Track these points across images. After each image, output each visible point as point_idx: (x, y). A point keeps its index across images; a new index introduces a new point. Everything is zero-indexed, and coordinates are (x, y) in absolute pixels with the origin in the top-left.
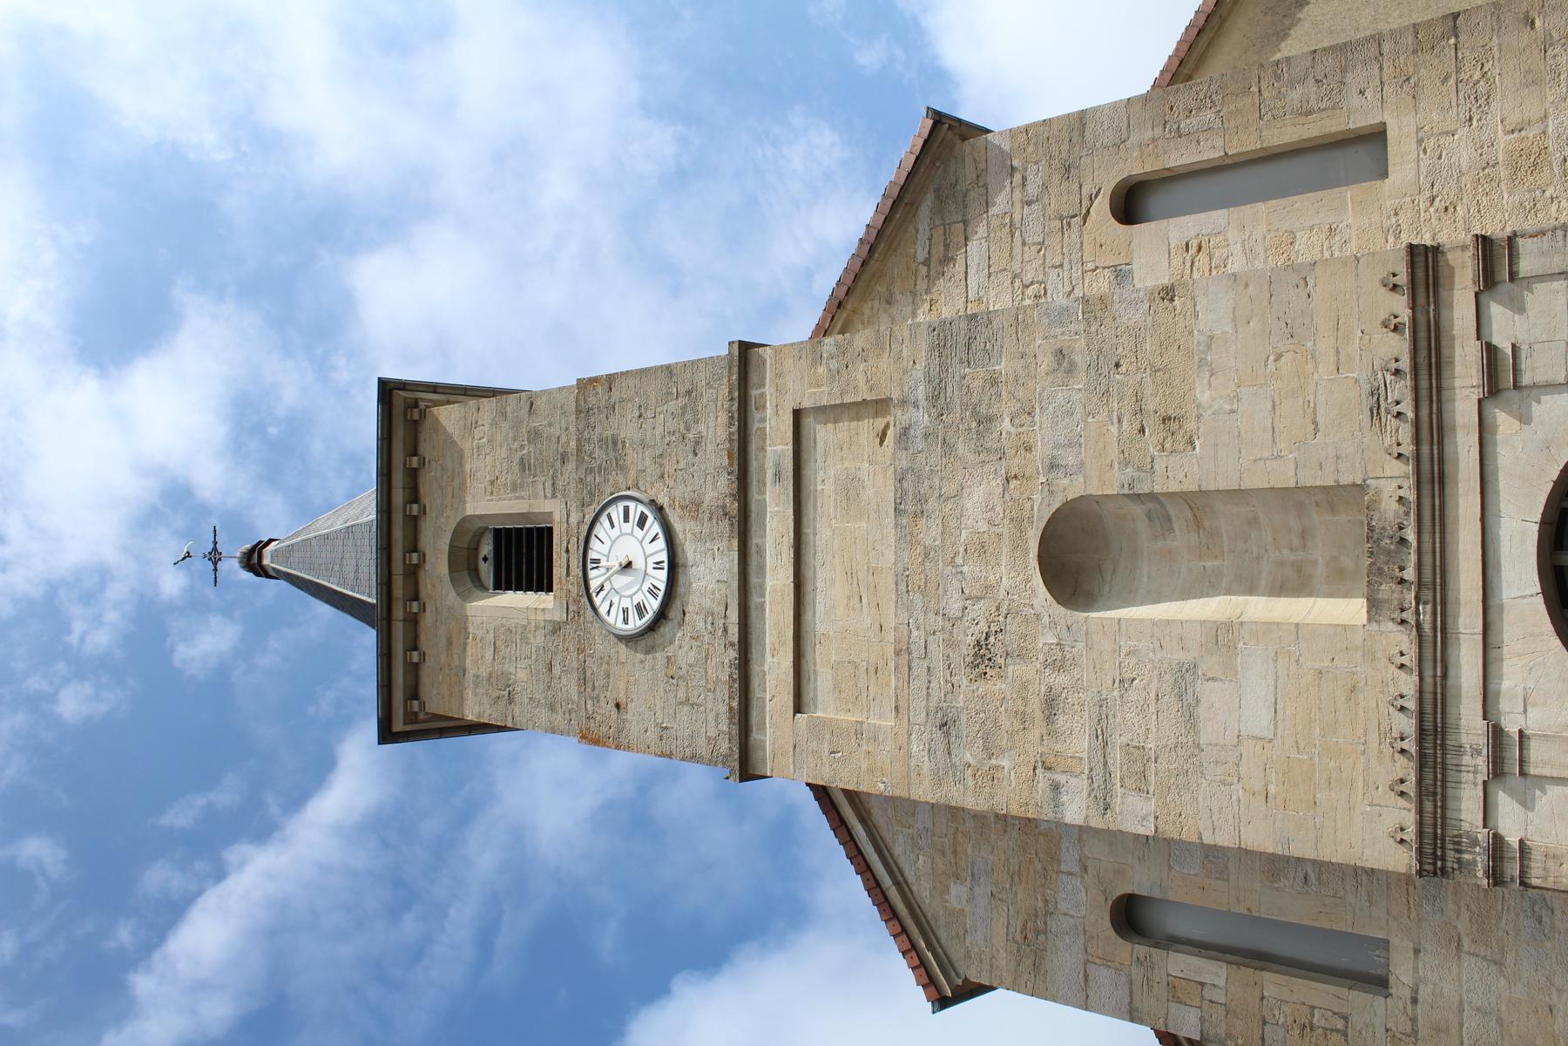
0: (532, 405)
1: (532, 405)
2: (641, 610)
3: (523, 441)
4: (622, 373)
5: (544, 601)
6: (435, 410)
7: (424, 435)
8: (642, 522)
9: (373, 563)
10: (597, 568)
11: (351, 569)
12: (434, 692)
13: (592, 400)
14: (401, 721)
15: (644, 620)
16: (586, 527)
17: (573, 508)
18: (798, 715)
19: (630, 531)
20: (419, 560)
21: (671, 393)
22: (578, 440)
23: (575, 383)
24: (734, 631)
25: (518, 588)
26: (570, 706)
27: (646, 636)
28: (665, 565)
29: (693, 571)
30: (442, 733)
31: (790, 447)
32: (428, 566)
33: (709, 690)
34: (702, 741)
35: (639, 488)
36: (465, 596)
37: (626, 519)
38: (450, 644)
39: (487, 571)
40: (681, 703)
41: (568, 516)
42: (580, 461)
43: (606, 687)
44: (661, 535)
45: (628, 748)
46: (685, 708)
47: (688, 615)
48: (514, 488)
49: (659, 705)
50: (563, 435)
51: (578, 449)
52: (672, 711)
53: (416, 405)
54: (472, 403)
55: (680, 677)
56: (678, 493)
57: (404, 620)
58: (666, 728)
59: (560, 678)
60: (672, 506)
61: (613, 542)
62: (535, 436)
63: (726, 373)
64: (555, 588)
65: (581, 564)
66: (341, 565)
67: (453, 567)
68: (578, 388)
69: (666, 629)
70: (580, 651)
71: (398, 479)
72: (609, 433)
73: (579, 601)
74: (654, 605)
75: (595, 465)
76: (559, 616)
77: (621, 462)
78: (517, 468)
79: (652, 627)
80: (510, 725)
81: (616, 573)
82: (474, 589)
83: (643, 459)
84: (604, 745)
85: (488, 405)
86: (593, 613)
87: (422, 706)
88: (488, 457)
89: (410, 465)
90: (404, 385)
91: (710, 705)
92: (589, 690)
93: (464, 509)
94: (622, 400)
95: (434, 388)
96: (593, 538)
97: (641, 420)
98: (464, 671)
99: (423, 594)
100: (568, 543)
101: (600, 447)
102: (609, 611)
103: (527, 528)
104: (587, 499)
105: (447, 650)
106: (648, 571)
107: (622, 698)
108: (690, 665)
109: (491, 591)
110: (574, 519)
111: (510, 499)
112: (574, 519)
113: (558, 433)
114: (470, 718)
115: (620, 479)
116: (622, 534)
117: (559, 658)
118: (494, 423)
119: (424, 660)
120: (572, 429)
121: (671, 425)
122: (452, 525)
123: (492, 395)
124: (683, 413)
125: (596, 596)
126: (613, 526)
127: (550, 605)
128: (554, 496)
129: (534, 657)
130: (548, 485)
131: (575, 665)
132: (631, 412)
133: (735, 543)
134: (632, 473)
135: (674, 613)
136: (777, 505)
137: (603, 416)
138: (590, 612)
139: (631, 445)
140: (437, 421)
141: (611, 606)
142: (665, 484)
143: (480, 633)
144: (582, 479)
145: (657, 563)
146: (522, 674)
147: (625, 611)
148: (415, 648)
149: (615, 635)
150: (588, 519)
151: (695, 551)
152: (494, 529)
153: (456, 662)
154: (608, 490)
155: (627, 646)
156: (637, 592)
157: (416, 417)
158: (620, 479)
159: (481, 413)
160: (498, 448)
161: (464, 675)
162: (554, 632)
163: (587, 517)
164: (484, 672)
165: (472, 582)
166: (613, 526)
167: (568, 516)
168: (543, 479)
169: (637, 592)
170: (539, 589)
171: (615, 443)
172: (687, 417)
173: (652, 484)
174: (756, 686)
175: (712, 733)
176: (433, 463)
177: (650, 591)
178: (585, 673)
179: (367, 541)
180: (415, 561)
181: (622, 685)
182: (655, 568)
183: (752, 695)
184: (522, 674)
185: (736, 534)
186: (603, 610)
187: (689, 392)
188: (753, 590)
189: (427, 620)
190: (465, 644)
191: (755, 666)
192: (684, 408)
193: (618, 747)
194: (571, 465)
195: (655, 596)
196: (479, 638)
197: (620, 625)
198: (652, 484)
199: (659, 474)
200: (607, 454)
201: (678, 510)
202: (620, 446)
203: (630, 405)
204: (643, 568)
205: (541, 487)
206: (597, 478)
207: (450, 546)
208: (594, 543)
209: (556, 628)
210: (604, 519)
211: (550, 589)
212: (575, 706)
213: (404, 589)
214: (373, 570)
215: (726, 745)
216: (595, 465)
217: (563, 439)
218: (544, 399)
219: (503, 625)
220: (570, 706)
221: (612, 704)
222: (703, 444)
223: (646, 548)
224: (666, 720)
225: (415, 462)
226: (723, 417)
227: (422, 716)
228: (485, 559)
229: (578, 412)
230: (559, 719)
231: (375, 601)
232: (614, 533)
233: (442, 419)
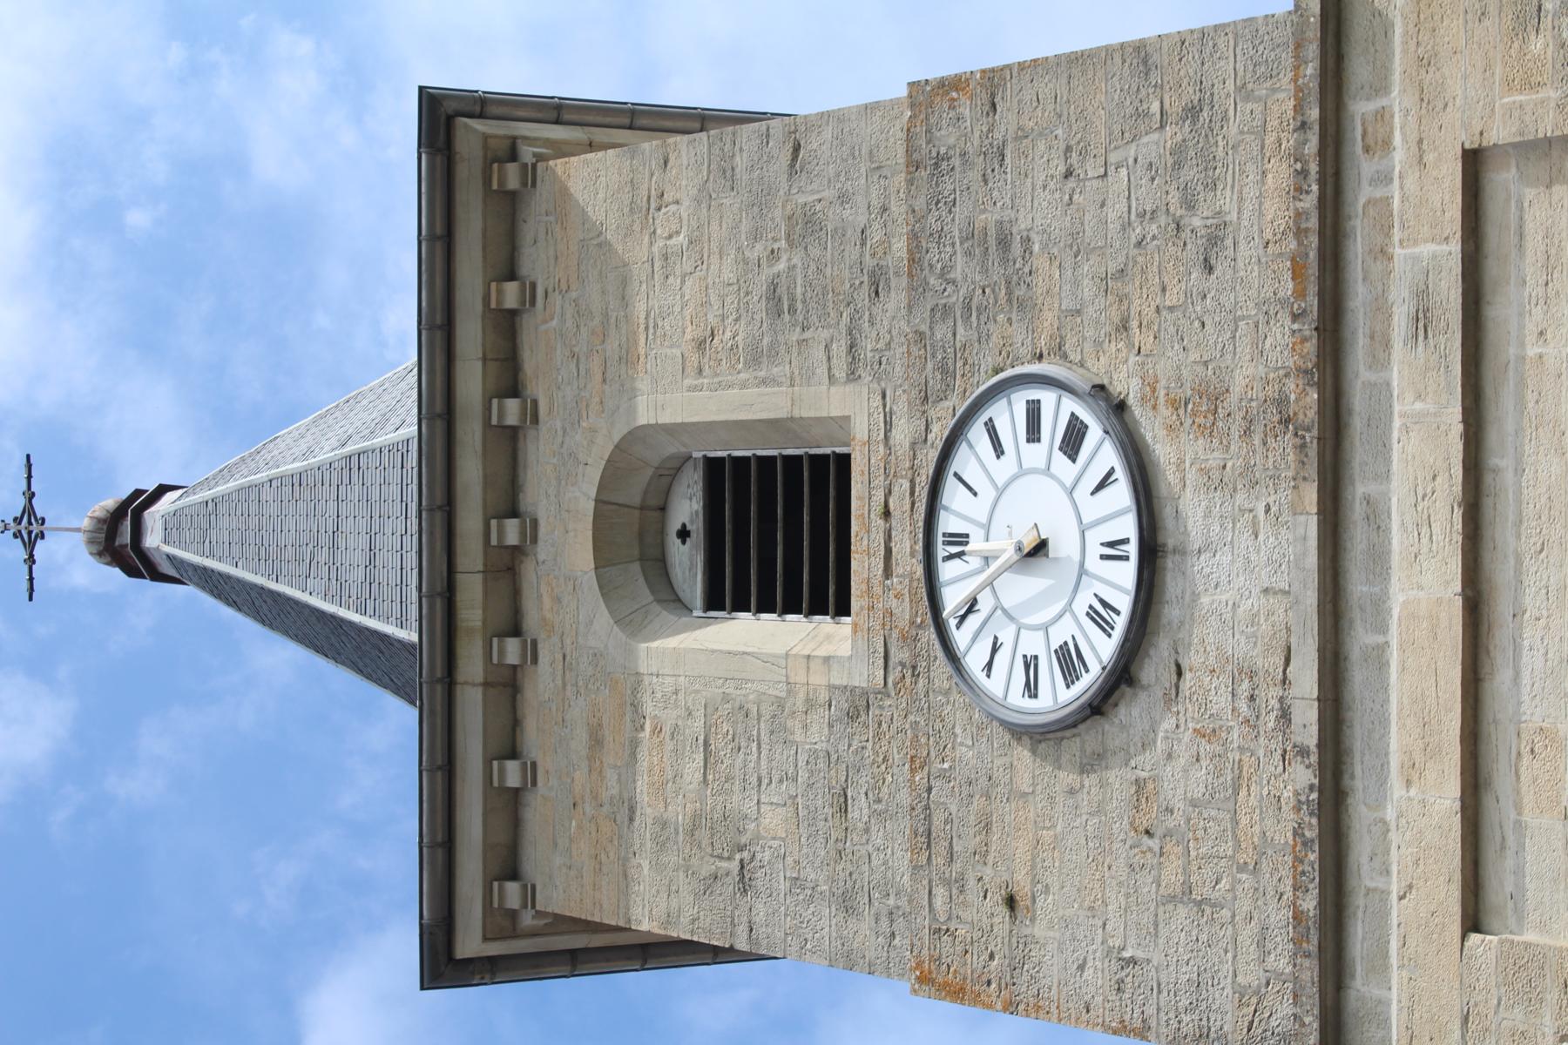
0: (797, 149)
1: (797, 149)
2: (1069, 661)
3: (775, 240)
4: (1022, 66)
5: (829, 637)
6: (558, 165)
7: (530, 229)
8: (1073, 440)
9: (411, 543)
10: (960, 555)
11: (359, 558)
12: (558, 860)
13: (947, 137)
15: (1079, 687)
16: (934, 455)
17: (900, 407)
18: (1475, 938)
19: (1042, 465)
20: (523, 534)
21: (1147, 114)
22: (914, 236)
23: (903, 92)
24: (1307, 719)
25: (766, 606)
26: (891, 902)
27: (1082, 727)
28: (1132, 549)
29: (1201, 566)
30: (575, 962)
31: (1455, 247)
32: (543, 551)
33: (1242, 868)
34: (1223, 997)
35: (1065, 356)
36: (633, 625)
37: (1033, 433)
38: (596, 742)
40: (1172, 899)
41: (888, 425)
42: (918, 288)
43: (982, 854)
44: (1121, 474)
45: (1037, 1009)
46: (1182, 911)
47: (1188, 676)
48: (755, 360)
49: (1115, 901)
50: (876, 226)
51: (912, 260)
52: (1147, 919)
53: (513, 155)
54: (649, 146)
55: (1168, 834)
56: (1163, 368)
57: (486, 684)
58: (1133, 961)
59: (867, 831)
60: (1151, 399)
61: (1001, 492)
62: (805, 226)
63: (1287, 59)
64: (855, 604)
65: (919, 547)
66: (334, 546)
67: (604, 556)
68: (912, 106)
69: (1132, 712)
70: (917, 763)
71: (471, 335)
72: (988, 218)
73: (916, 639)
74: (1101, 649)
75: (955, 298)
76: (865, 675)
77: (1021, 291)
78: (760, 308)
79: (1098, 706)
80: (742, 945)
81: (1009, 568)
82: (656, 608)
83: (1077, 283)
84: (976, 1000)
85: (686, 150)
86: (949, 669)
87: (529, 895)
88: (688, 283)
89: (499, 302)
90: (481, 105)
91: (1244, 906)
92: (938, 861)
93: (632, 411)
94: (1022, 135)
95: (556, 111)
96: (950, 483)
97: (1071, 183)
98: (632, 810)
99: (531, 621)
100: (889, 493)
101: (969, 254)
102: (989, 665)
103: (786, 458)
104: (935, 384)
105: (590, 759)
106: (1088, 565)
107: (1022, 886)
108: (1194, 804)
109: (696, 613)
110: (903, 433)
111: (743, 386)
112: (903, 433)
113: (862, 220)
114: (645, 927)
115: (1018, 334)
116: (1022, 472)
117: (864, 780)
118: (704, 197)
119: (534, 783)
120: (898, 209)
121: (1147, 196)
122: (603, 450)
123: (697, 125)
124: (1178, 165)
126: (999, 450)
127: (844, 648)
128: (853, 376)
129: (803, 775)
130: (840, 349)
131: (904, 797)
132: (1046, 162)
133: (1311, 494)
134: (1049, 318)
135: (1153, 670)
136: (1419, 397)
137: (974, 175)
138: (942, 665)
139: (1044, 247)
140: (565, 193)
141: (994, 650)
142: (1130, 345)
143: (670, 717)
144: (921, 335)
145: (1111, 544)
146: (773, 820)
147: (1031, 664)
148: (513, 753)
149: (1003, 723)
150: (939, 433)
151: (1208, 514)
152: (705, 456)
153: (611, 787)
154: (989, 362)
155: (1034, 752)
156: (1060, 616)
157: (513, 183)
158: (1018, 334)
159: (673, 172)
160: (715, 259)
161: (631, 820)
162: (852, 715)
163: (935, 428)
164: (679, 813)
165: (653, 592)
166: (999, 450)
167: (888, 425)
168: (825, 334)
169: (1060, 616)
170: (818, 607)
171: (1004, 243)
172: (1189, 173)
173: (1098, 344)
174: (1364, 860)
175: (1251, 976)
176: (556, 299)
177: (1093, 615)
178: (929, 818)
179: (395, 489)
180: (512, 538)
181: (1021, 848)
182: (1104, 557)
183: (1352, 882)
184: (773, 820)
185: (1312, 470)
186: (974, 662)
187: (1192, 112)
188: (1356, 614)
189: (542, 685)
190: (634, 744)
191: (1363, 809)
192: (1179, 151)
193: (1011, 1007)
194: (895, 299)
195: (1105, 627)
196: (667, 730)
197: (1017, 698)
198: (1098, 344)
199: (1117, 320)
200: (985, 271)
201: (1165, 411)
202: (1017, 249)
203: (1041, 145)
204: (1077, 557)
205: (819, 353)
206: (961, 330)
207: (596, 501)
208: (953, 494)
209: (857, 706)
210: (977, 433)
211: (843, 609)
212: (903, 902)
213: (485, 610)
214: (411, 559)
215: (1286, 1009)
216: (955, 298)
217: (876, 235)
218: (828, 134)
219: (726, 698)
220: (891, 902)
221: (995, 902)
222: (1229, 242)
224: (1132, 941)
225: (511, 294)
226: (1280, 174)
227: (527, 920)
228: (684, 534)
229: (914, 165)
230: (864, 932)
231: (414, 638)
232: (1003, 468)
233: (577, 188)
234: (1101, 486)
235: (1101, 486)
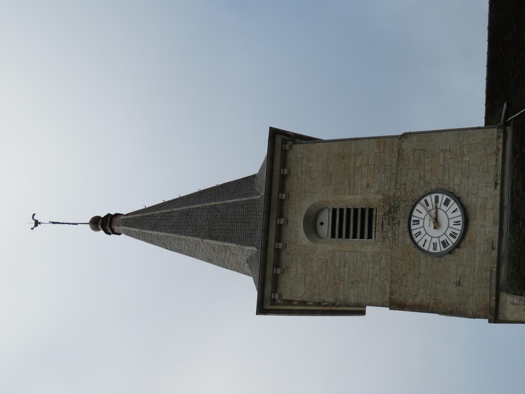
2: (444, 244)
8: (447, 203)
15: (446, 249)
44: (458, 209)
87: (280, 296)
125: (416, 238)
141: (425, 242)
177: (451, 235)
182: (454, 225)
186: (421, 244)
208: (415, 213)
227: (279, 301)
234: (454, 211)
235: (454, 211)
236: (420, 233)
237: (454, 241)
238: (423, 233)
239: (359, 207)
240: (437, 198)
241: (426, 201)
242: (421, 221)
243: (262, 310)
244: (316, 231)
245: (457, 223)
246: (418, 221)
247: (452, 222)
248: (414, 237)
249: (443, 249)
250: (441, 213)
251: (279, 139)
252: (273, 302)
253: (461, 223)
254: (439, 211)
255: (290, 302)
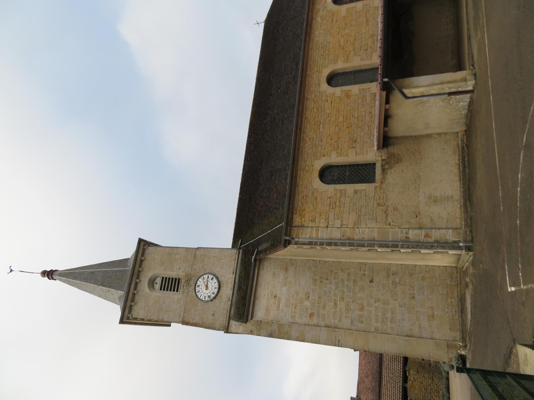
2: (209, 297)
8: (212, 279)
14: (126, 319)
39: (157, 286)
44: (217, 282)
102: (201, 296)
177: (212, 293)
186: (199, 296)
208: (198, 282)
223: (213, 285)
227: (131, 318)
236: (199, 291)
237: (213, 296)
238: (201, 291)
239: (174, 277)
240: (208, 277)
241: (204, 277)
242: (201, 286)
243: (122, 321)
244: (153, 286)
245: (215, 288)
246: (199, 286)
247: (213, 287)
248: (197, 293)
249: (208, 299)
250: (209, 283)
251: (142, 243)
252: (128, 318)
253: (217, 288)
254: (209, 282)
255: (136, 319)
